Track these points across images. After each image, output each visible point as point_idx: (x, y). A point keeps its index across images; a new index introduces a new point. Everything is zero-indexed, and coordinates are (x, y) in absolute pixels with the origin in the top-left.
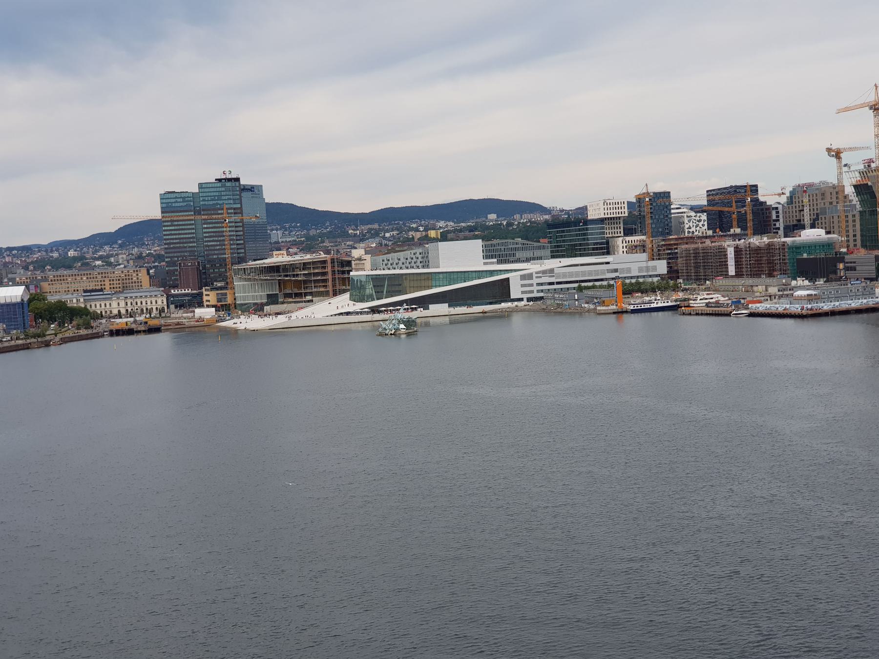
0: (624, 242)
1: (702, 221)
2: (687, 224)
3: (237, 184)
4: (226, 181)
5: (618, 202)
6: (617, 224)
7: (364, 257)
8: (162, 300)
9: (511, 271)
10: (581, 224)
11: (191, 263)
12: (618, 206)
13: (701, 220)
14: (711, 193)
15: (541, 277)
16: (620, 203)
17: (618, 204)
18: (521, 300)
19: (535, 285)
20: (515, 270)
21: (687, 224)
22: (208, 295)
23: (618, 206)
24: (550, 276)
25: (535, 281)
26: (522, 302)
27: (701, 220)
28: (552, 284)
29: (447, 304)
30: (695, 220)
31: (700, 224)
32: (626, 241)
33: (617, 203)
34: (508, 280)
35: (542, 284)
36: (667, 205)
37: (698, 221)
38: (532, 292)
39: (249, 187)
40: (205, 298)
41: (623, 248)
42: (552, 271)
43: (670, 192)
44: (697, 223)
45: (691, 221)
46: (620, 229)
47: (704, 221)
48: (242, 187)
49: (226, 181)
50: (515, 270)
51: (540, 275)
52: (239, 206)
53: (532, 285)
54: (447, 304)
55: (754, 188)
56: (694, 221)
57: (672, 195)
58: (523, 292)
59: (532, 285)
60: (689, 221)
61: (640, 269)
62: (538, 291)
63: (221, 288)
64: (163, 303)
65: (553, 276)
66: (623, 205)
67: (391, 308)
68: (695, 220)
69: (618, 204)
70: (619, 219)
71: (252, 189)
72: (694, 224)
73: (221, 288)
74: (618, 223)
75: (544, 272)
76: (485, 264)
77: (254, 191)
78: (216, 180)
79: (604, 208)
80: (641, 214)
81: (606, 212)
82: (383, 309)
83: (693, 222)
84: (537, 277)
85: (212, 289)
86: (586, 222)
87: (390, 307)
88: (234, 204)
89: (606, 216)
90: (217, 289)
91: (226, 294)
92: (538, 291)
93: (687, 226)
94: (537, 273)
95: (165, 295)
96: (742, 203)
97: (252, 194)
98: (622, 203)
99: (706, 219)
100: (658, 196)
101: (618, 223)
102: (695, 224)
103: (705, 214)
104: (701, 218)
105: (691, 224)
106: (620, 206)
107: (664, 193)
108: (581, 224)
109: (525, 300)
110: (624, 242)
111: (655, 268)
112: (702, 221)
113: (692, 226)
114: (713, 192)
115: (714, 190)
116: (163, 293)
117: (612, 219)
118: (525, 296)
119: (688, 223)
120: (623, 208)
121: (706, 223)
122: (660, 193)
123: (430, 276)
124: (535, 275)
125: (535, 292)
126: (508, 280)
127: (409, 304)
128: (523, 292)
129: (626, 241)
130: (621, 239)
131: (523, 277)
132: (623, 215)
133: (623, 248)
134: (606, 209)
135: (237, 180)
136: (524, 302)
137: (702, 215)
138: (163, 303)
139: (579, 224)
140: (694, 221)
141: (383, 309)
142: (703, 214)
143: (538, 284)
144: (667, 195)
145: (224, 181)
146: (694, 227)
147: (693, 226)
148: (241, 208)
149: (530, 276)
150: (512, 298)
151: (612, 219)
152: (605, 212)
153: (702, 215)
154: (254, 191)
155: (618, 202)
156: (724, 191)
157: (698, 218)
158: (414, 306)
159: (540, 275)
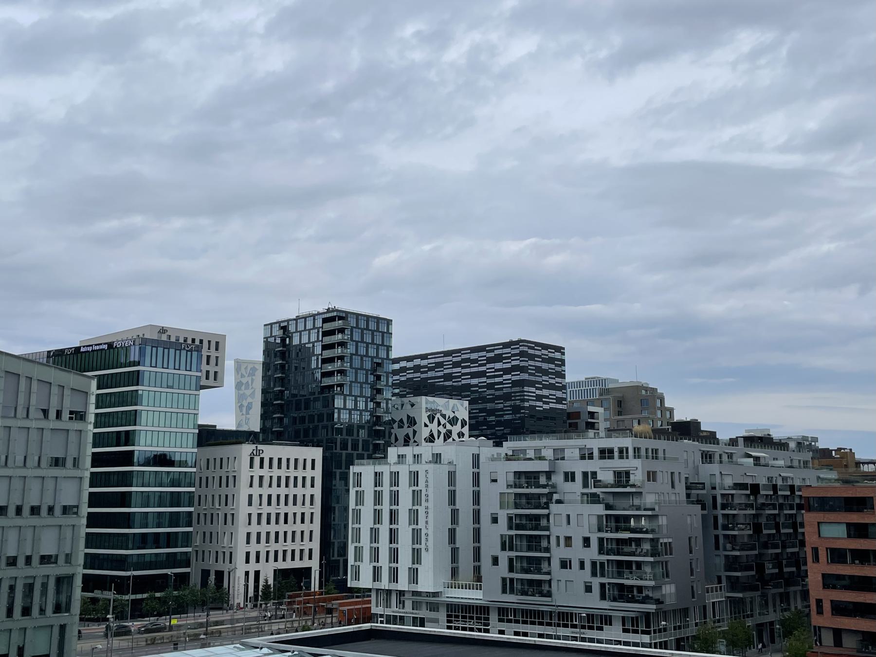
0: (257, 460)
1: (459, 423)
2: (426, 425)
13: (457, 419)
14: (410, 365)
21: (426, 425)
27: (457, 419)
30: (444, 416)
31: (456, 429)
32: (262, 460)
36: (383, 359)
37: (449, 422)
41: (251, 486)
43: (391, 321)
44: (449, 427)
45: (436, 420)
47: (463, 424)
55: (557, 355)
56: (443, 421)
57: (394, 329)
60: (431, 418)
68: (444, 416)
72: (441, 428)
83: (439, 424)
93: (425, 433)
96: (537, 388)
99: (467, 419)
100: (362, 324)
102: (443, 431)
103: (466, 403)
104: (457, 414)
105: (434, 427)
107: (378, 320)
110: (257, 460)
112: (459, 423)
113: (436, 436)
114: (417, 362)
115: (423, 357)
119: (428, 423)
121: (466, 430)
122: (368, 318)
129: (262, 460)
130: (247, 449)
133: (251, 486)
137: (459, 406)
140: (443, 421)
142: (462, 405)
146: (442, 436)
147: (439, 433)
153: (459, 406)
156: (474, 356)
157: (449, 414)
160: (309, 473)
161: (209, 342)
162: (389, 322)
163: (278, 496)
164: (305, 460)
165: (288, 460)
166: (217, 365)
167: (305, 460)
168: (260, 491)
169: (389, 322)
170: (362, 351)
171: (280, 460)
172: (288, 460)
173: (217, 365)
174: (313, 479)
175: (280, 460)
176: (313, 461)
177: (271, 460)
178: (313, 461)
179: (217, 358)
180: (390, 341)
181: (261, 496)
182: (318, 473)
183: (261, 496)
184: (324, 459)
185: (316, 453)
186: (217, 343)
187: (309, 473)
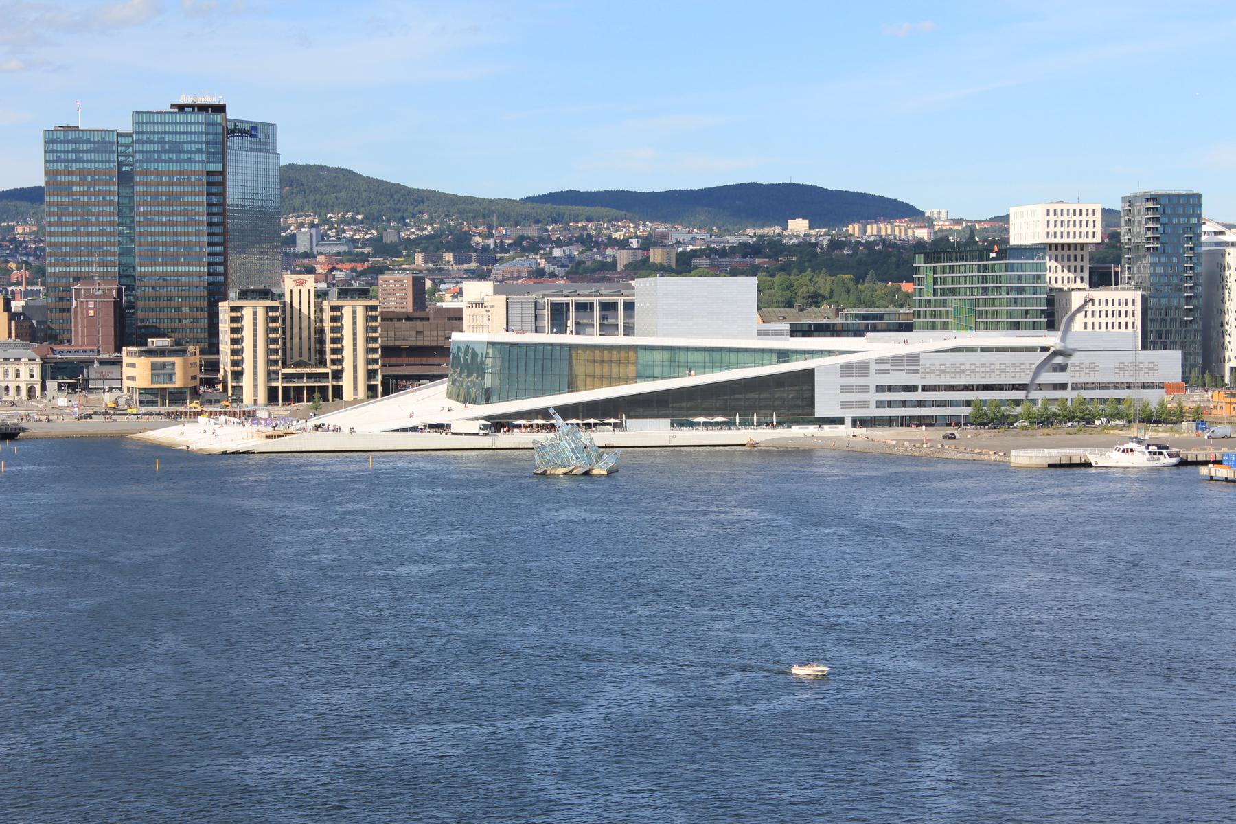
3: (217, 118)
4: (193, 110)
5: (1081, 211)
6: (1075, 260)
7: (489, 301)
8: (32, 371)
9: (821, 353)
10: (993, 255)
11: (104, 290)
12: (1081, 218)
15: (886, 372)
16: (1084, 213)
17: (1081, 214)
18: (839, 421)
19: (873, 389)
20: (830, 353)
22: (132, 365)
23: (1081, 218)
24: (909, 372)
25: (874, 380)
26: (841, 427)
28: (911, 388)
29: (668, 421)
33: (1078, 213)
34: (808, 376)
35: (892, 388)
38: (864, 404)
39: (247, 127)
40: (126, 371)
42: (913, 359)
46: (1082, 271)
48: (231, 127)
49: (193, 110)
50: (830, 353)
51: (887, 367)
52: (219, 167)
53: (865, 389)
54: (668, 421)
58: (844, 405)
59: (865, 389)
61: (1121, 369)
62: (880, 404)
63: (162, 352)
64: (32, 376)
65: (917, 372)
66: (1092, 218)
67: (540, 422)
69: (1081, 214)
70: (1082, 249)
71: (253, 132)
73: (162, 352)
74: (1079, 258)
75: (896, 361)
76: (762, 333)
77: (256, 136)
78: (173, 106)
79: (1048, 222)
80: (1132, 241)
81: (1052, 230)
82: (522, 422)
84: (880, 372)
85: (141, 353)
86: (1006, 251)
87: (537, 418)
88: (208, 162)
89: (1052, 241)
90: (151, 353)
91: (173, 364)
92: (880, 404)
94: (880, 361)
95: (38, 360)
97: (251, 142)
98: (1091, 213)
100: (1175, 201)
101: (1079, 258)
106: (1084, 218)
108: (993, 255)
109: (848, 421)
111: (1153, 368)
116: (33, 355)
117: (1066, 248)
118: (849, 414)
120: (1091, 224)
122: (1179, 196)
123: (632, 354)
124: (873, 367)
125: (873, 404)
126: (810, 373)
127: (581, 416)
128: (844, 405)
131: (847, 370)
132: (1091, 240)
134: (1052, 224)
135: (220, 109)
136: (845, 431)
138: (32, 376)
139: (988, 256)
141: (522, 422)
143: (880, 389)
144: (1189, 204)
145: (190, 109)
148: (223, 173)
149: (862, 369)
150: (819, 412)
151: (1066, 248)
152: (1049, 230)
154: (256, 136)
155: (1081, 211)
158: (592, 421)
159: (887, 367)
160: (1130, 308)
161: (1087, 210)
162: (1199, 196)
163: (1107, 324)
164: (1126, 300)
165: (1113, 300)
166: (1094, 226)
167: (1126, 300)
168: (1093, 320)
169: (1199, 196)
170: (1175, 221)
171: (1107, 300)
172: (1113, 300)
173: (1094, 226)
174: (1133, 313)
175: (1107, 300)
176: (1133, 300)
177: (1100, 300)
178: (1133, 300)
179: (1094, 222)
180: (1201, 210)
181: (1093, 323)
182: (1138, 308)
183: (1093, 323)
184: (1143, 296)
185: (1138, 295)
186: (1094, 210)
187: (1130, 308)
